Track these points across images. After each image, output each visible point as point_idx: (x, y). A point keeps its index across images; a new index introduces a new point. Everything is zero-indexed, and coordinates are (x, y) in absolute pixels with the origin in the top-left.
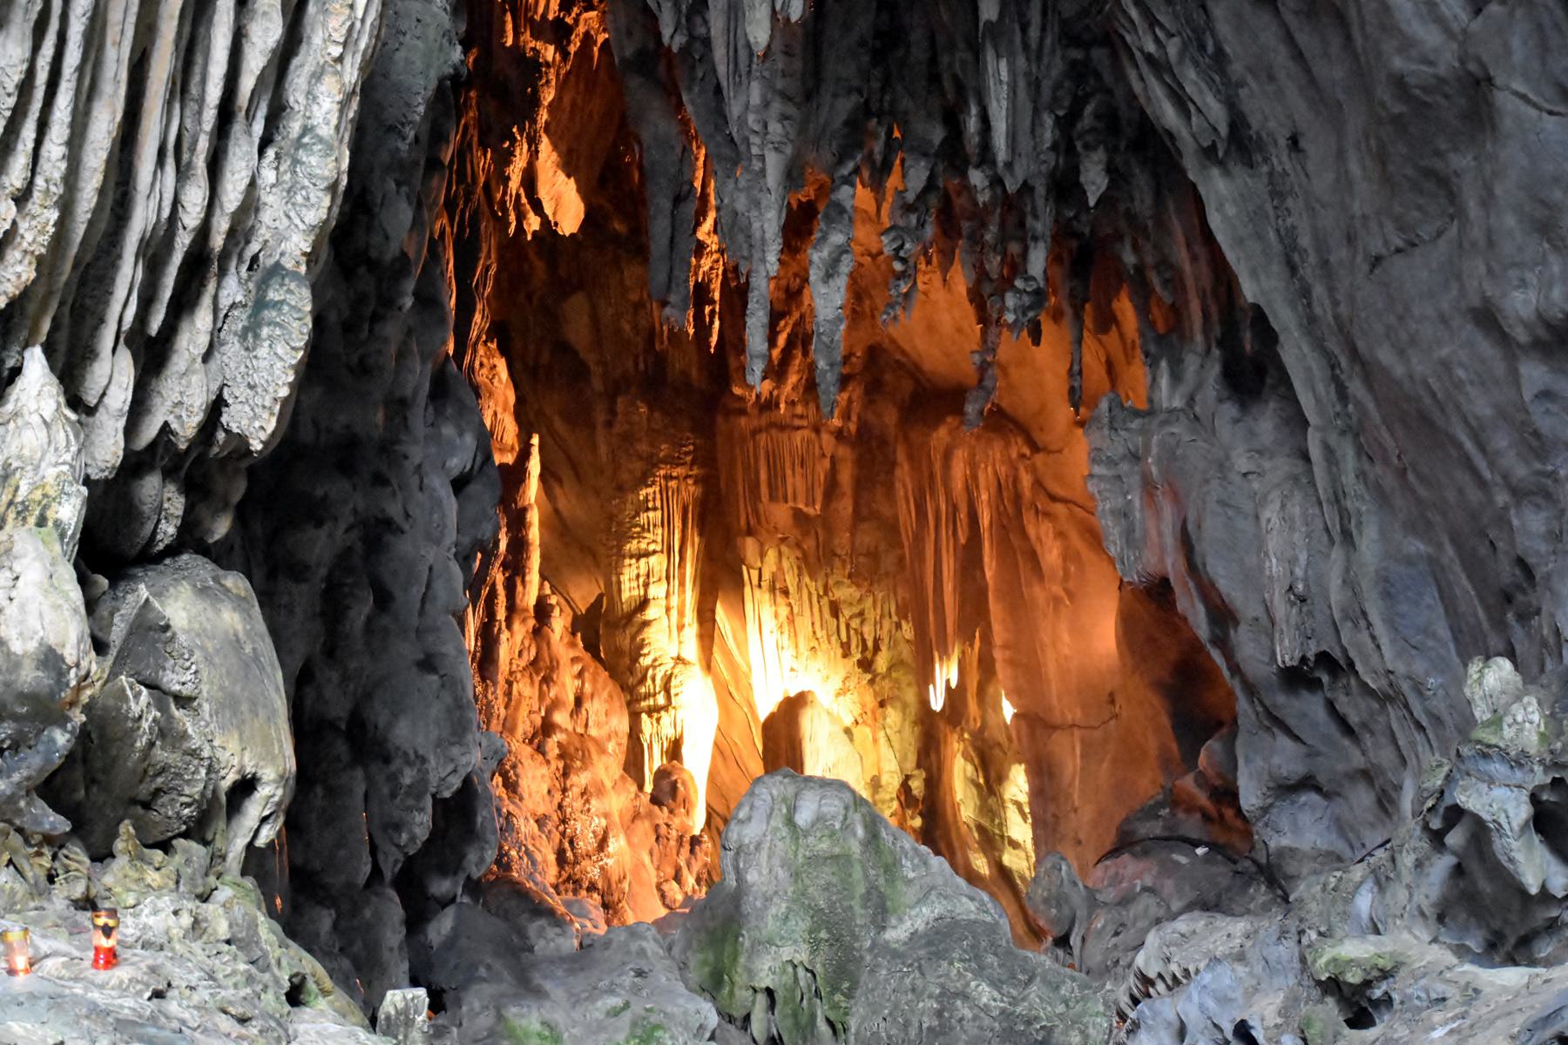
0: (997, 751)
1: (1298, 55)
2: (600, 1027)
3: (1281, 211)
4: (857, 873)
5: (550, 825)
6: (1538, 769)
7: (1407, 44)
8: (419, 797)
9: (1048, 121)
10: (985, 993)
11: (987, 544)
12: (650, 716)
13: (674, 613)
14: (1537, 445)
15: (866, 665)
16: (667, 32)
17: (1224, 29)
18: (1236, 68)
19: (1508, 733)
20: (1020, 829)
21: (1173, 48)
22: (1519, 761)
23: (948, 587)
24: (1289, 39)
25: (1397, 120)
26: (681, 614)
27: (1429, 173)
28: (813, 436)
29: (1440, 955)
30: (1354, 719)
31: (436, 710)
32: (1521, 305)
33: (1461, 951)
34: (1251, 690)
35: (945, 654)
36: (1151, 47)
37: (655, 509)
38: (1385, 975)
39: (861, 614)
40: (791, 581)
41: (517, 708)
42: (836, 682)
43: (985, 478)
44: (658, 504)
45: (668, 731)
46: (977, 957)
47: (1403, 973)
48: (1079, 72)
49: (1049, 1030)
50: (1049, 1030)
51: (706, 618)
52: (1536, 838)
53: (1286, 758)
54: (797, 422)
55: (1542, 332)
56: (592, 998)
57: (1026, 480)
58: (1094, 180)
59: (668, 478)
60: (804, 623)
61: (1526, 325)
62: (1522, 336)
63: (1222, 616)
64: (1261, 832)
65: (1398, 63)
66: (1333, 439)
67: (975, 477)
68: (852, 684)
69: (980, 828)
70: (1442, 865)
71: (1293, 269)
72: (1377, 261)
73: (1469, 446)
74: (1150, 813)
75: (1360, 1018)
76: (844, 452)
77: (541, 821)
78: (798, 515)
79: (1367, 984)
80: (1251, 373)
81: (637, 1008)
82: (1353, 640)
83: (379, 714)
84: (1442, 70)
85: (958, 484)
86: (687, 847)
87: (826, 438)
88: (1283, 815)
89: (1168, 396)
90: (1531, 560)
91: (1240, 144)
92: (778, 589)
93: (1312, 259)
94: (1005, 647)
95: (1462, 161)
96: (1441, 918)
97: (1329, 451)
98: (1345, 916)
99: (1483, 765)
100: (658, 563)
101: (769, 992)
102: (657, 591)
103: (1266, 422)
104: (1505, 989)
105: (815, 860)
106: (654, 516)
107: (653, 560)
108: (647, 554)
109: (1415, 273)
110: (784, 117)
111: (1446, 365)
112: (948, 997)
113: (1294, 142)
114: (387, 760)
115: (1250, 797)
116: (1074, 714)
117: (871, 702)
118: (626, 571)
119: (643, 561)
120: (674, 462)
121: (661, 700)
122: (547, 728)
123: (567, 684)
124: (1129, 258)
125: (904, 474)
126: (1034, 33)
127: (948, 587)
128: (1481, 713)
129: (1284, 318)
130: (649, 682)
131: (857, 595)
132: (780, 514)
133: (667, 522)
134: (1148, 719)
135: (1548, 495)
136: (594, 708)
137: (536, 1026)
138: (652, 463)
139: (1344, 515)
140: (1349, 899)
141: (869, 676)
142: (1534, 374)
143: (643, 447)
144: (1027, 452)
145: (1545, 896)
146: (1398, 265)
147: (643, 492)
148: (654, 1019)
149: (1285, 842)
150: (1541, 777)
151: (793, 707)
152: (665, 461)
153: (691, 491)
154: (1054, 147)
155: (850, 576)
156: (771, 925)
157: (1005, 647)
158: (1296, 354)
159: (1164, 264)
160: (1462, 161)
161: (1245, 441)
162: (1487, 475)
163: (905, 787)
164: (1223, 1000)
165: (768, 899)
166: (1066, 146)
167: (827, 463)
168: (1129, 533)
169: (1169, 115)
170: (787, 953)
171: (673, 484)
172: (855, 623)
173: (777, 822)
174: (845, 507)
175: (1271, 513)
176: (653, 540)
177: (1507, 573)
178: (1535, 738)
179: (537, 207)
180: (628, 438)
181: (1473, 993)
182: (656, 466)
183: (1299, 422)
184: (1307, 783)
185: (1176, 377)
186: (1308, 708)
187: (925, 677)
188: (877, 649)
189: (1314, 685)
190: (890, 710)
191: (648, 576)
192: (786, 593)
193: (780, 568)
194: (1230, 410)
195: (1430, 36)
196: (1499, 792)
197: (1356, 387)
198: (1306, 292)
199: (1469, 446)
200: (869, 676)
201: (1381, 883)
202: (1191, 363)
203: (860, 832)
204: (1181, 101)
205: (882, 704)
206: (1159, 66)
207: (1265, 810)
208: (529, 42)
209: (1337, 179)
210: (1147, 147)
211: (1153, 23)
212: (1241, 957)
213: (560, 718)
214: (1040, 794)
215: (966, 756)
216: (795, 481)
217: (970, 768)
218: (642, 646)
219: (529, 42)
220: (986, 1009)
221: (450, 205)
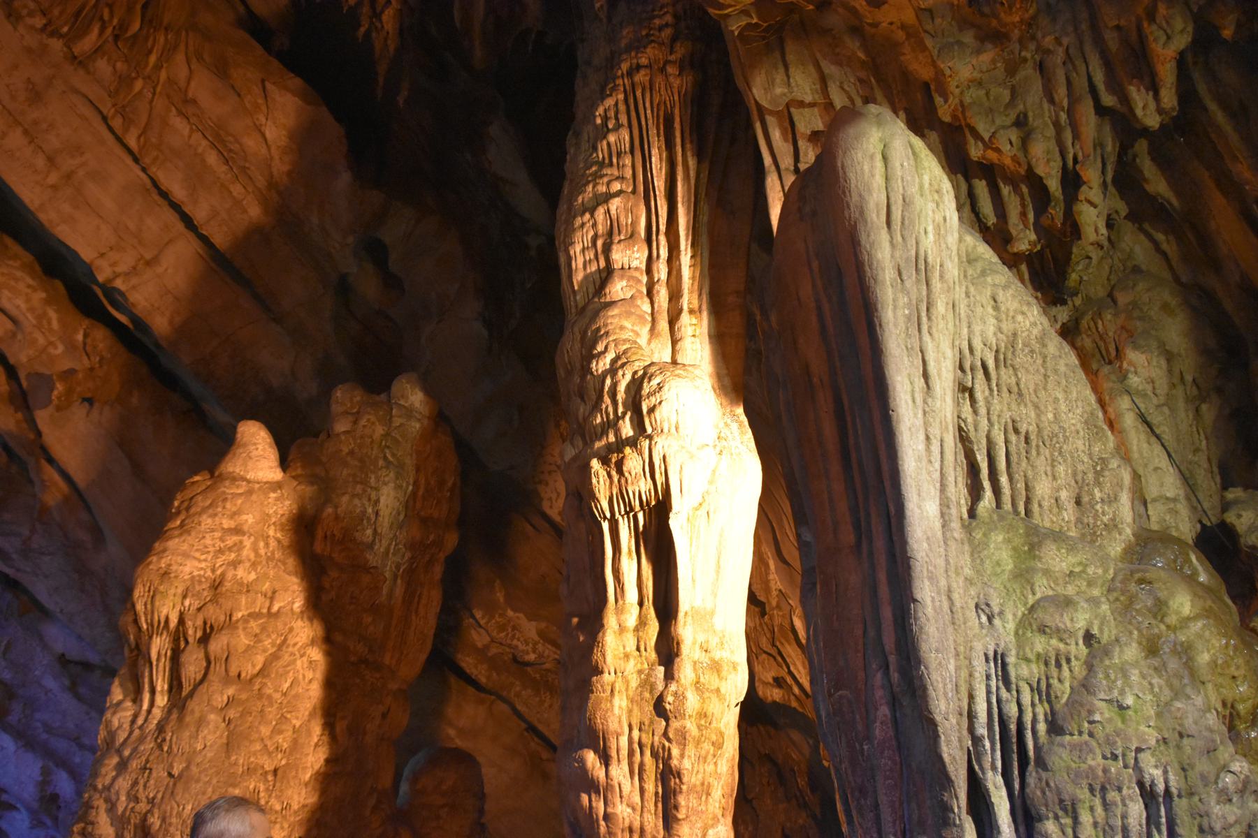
12: (605, 461)
13: (662, 295)
26: (675, 295)
37: (618, 126)
44: (623, 119)
45: (641, 487)
102: (630, 256)
107: (615, 204)
108: (608, 197)
118: (578, 236)
119: (600, 212)
120: (638, 45)
121: (627, 430)
130: (607, 400)
133: (640, 148)
147: (601, 110)
152: (628, 49)
153: (677, 84)
171: (641, 77)
188: (1072, 181)
191: (610, 234)
218: (596, 340)
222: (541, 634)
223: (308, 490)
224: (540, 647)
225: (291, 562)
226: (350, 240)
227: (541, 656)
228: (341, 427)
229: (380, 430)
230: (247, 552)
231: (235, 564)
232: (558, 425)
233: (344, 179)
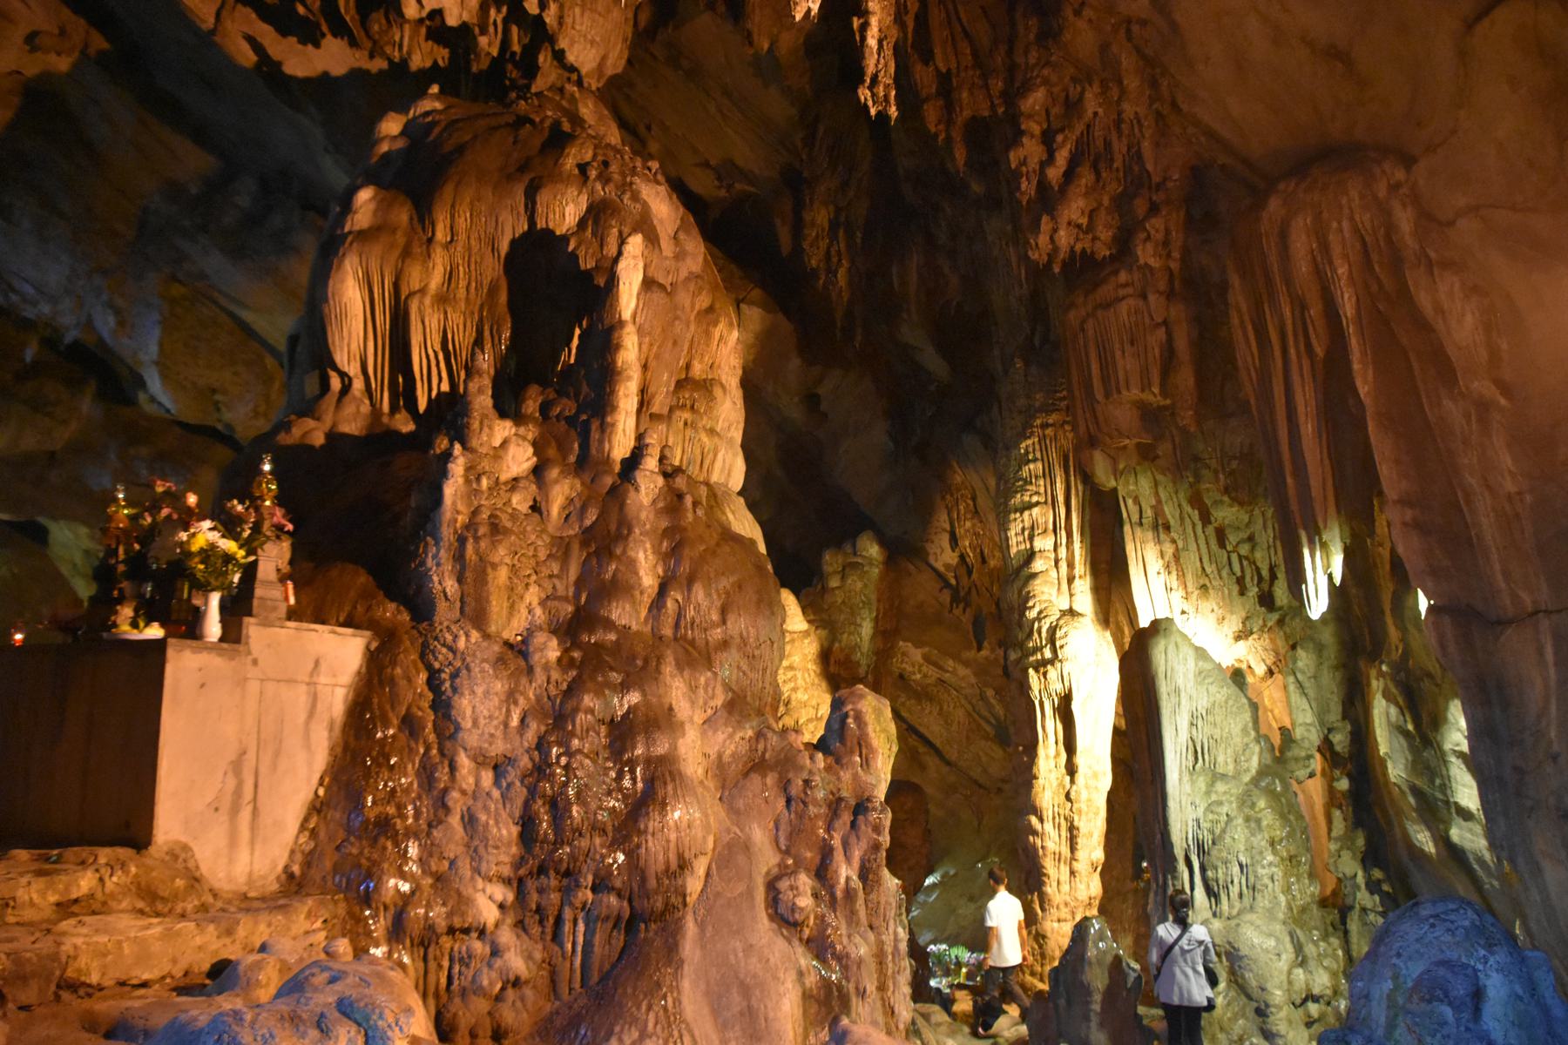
0: (1426, 685)
5: (513, 775)
11: (1354, 342)
12: (1037, 671)
13: (1063, 566)
20: (1467, 793)
23: (1308, 429)
26: (1071, 565)
28: (1141, 303)
35: (1315, 534)
37: (1035, 460)
39: (1251, 539)
41: (481, 579)
42: (1234, 624)
44: (1038, 455)
45: (1056, 686)
54: (1122, 292)
57: (1405, 220)
59: (1044, 426)
60: (1191, 560)
67: (1325, 247)
68: (1256, 625)
69: (1416, 791)
76: (1177, 311)
85: (1303, 268)
86: (846, 817)
92: (1160, 527)
94: (1404, 502)
102: (1044, 543)
107: (1035, 511)
108: (1030, 506)
117: (1282, 646)
118: (1012, 526)
119: (1026, 513)
120: (1047, 409)
121: (1048, 654)
127: (1308, 429)
130: (1036, 635)
131: (1246, 518)
132: (1122, 414)
133: (1048, 474)
138: (1029, 414)
141: (1275, 616)
143: (1022, 402)
144: (1400, 175)
147: (1023, 445)
152: (1040, 410)
155: (1226, 491)
157: (1404, 502)
163: (1326, 747)
167: (1161, 333)
171: (1049, 431)
172: (1244, 549)
174: (1185, 378)
182: (1034, 417)
188: (1273, 577)
190: (1300, 652)
191: (1032, 528)
192: (1167, 528)
193: (1159, 502)
200: (1275, 616)
205: (1293, 647)
215: (1387, 695)
216: (1126, 364)
217: (1393, 710)
218: (1027, 599)
222: (926, 658)
223: (823, 633)
224: (924, 669)
225: (824, 684)
226: (796, 399)
227: (925, 676)
228: (834, 583)
229: (859, 585)
230: (800, 682)
231: (795, 690)
232: (943, 498)
233: (795, 363)
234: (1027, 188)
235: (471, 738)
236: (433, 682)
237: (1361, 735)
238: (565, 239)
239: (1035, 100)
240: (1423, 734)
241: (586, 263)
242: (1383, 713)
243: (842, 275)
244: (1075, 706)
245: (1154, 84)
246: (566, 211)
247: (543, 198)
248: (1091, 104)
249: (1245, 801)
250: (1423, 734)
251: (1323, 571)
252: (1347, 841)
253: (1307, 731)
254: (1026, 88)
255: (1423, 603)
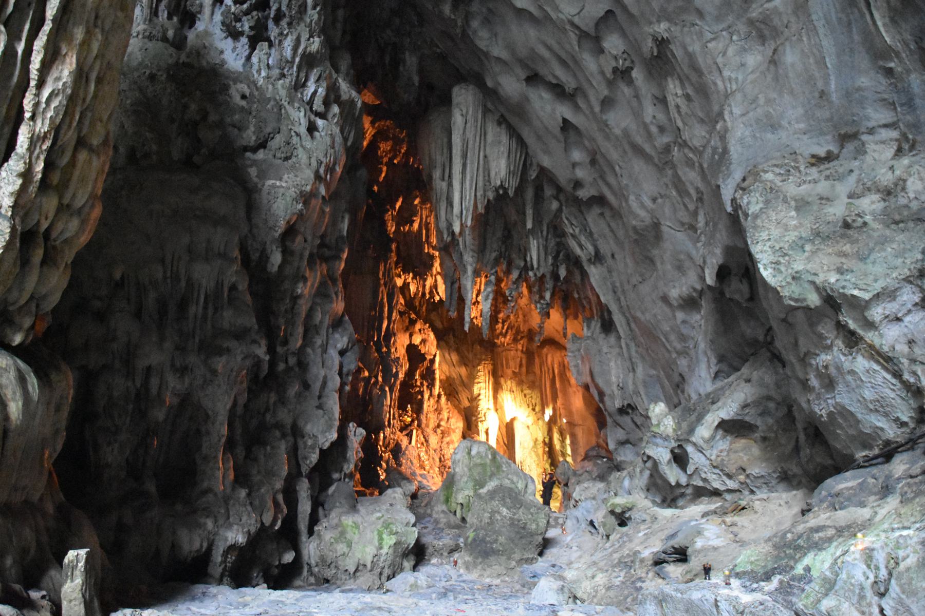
1: (612, 231)
2: (374, 523)
3: (611, 276)
4: (488, 469)
6: (673, 441)
7: (636, 216)
8: (314, 449)
9: (550, 258)
10: (505, 511)
14: (683, 338)
15: (534, 410)
16: (445, 236)
17: (592, 225)
18: (596, 236)
19: (662, 428)
20: (569, 451)
21: (577, 230)
22: (666, 438)
23: (548, 389)
24: (609, 226)
25: (636, 241)
27: (647, 257)
29: (648, 503)
30: (639, 423)
31: (322, 421)
32: (674, 293)
33: (654, 502)
34: (610, 416)
36: (571, 231)
38: (630, 509)
40: (514, 389)
42: (526, 414)
43: (556, 362)
46: (503, 500)
47: (635, 509)
48: (558, 244)
49: (526, 524)
50: (526, 524)
51: (495, 398)
52: (674, 465)
53: (621, 434)
55: (681, 302)
56: (372, 514)
58: (563, 273)
60: (518, 399)
61: (676, 300)
62: (676, 304)
63: (601, 394)
64: (615, 456)
65: (634, 222)
66: (628, 342)
70: (647, 473)
71: (615, 292)
72: (635, 286)
73: (664, 340)
74: (592, 449)
75: (622, 524)
76: (524, 356)
77: (435, 451)
78: (514, 372)
79: (624, 512)
80: (608, 326)
81: (385, 517)
82: (636, 401)
83: (301, 423)
84: (647, 223)
87: (519, 353)
88: (621, 450)
89: (586, 332)
90: (684, 374)
91: (598, 258)
92: (512, 391)
93: (620, 289)
95: (655, 252)
96: (648, 490)
97: (627, 345)
98: (621, 487)
99: (654, 440)
100: (483, 385)
101: (462, 504)
102: (482, 392)
103: (612, 339)
104: (665, 518)
105: (476, 465)
106: (482, 373)
109: (645, 289)
110: (473, 257)
111: (655, 315)
112: (493, 513)
113: (613, 256)
114: (303, 437)
115: (612, 446)
116: (580, 422)
122: (439, 426)
123: (445, 415)
124: (576, 296)
125: (537, 360)
126: (545, 233)
127: (548, 389)
128: (654, 421)
129: (613, 307)
132: (509, 372)
133: (485, 375)
134: (591, 423)
135: (687, 354)
136: (452, 421)
137: (350, 523)
139: (632, 363)
140: (622, 482)
142: (680, 315)
145: (678, 485)
146: (641, 287)
148: (390, 521)
149: (623, 458)
150: (674, 444)
151: (513, 420)
153: (490, 367)
154: (552, 265)
156: (462, 484)
158: (618, 318)
159: (587, 297)
160: (655, 252)
161: (606, 344)
162: (669, 347)
163: (544, 441)
164: (588, 512)
165: (462, 477)
166: (555, 265)
168: (578, 372)
169: (578, 251)
170: (466, 493)
173: (465, 454)
174: (524, 369)
175: (612, 364)
176: (481, 379)
177: (677, 379)
178: (671, 430)
179: (438, 293)
180: (475, 355)
181: (655, 518)
183: (619, 338)
184: (627, 442)
185: (589, 327)
186: (626, 420)
187: (543, 413)
189: (628, 413)
194: (603, 336)
195: (642, 213)
196: (660, 449)
197: (633, 325)
198: (619, 300)
199: (664, 340)
201: (631, 477)
202: (593, 323)
203: (490, 456)
204: (581, 246)
206: (573, 236)
207: (616, 449)
208: (431, 251)
209: (625, 264)
210: (575, 263)
211: (572, 224)
212: (594, 498)
213: (443, 423)
214: (573, 444)
216: (511, 363)
219: (431, 251)
220: (505, 517)
221: (385, 284)
234: (498, 331)
235: (431, 446)
236: (424, 437)
237: (551, 439)
238: (417, 346)
239: (501, 315)
240: (563, 441)
241: (423, 352)
242: (556, 436)
243: (424, 308)
244: (489, 432)
245: (524, 316)
246: (417, 340)
247: (413, 337)
248: (512, 317)
249: (530, 453)
250: (563, 441)
251: (549, 412)
252: (547, 461)
253: (541, 439)
254: (499, 312)
255: (565, 421)
